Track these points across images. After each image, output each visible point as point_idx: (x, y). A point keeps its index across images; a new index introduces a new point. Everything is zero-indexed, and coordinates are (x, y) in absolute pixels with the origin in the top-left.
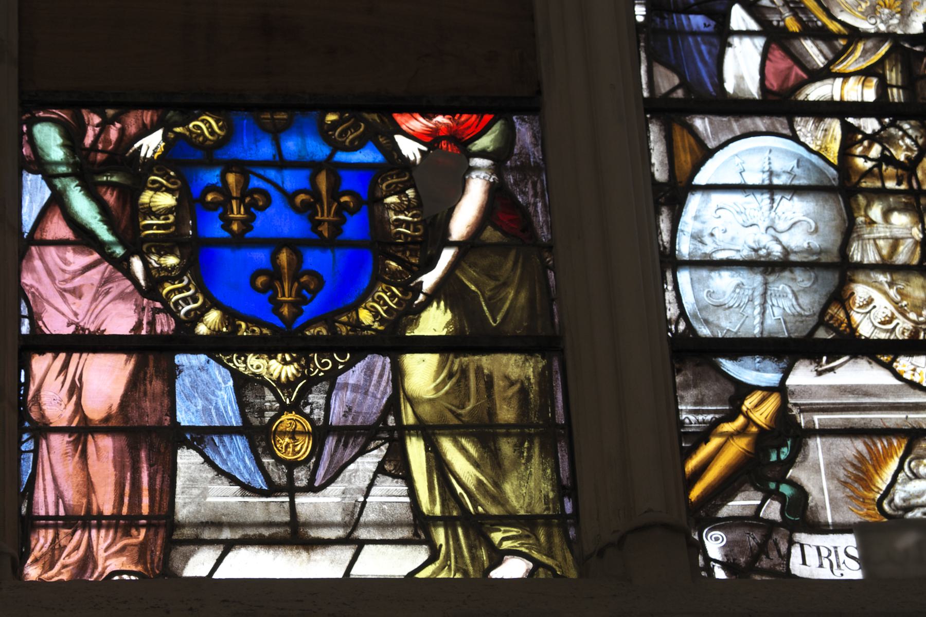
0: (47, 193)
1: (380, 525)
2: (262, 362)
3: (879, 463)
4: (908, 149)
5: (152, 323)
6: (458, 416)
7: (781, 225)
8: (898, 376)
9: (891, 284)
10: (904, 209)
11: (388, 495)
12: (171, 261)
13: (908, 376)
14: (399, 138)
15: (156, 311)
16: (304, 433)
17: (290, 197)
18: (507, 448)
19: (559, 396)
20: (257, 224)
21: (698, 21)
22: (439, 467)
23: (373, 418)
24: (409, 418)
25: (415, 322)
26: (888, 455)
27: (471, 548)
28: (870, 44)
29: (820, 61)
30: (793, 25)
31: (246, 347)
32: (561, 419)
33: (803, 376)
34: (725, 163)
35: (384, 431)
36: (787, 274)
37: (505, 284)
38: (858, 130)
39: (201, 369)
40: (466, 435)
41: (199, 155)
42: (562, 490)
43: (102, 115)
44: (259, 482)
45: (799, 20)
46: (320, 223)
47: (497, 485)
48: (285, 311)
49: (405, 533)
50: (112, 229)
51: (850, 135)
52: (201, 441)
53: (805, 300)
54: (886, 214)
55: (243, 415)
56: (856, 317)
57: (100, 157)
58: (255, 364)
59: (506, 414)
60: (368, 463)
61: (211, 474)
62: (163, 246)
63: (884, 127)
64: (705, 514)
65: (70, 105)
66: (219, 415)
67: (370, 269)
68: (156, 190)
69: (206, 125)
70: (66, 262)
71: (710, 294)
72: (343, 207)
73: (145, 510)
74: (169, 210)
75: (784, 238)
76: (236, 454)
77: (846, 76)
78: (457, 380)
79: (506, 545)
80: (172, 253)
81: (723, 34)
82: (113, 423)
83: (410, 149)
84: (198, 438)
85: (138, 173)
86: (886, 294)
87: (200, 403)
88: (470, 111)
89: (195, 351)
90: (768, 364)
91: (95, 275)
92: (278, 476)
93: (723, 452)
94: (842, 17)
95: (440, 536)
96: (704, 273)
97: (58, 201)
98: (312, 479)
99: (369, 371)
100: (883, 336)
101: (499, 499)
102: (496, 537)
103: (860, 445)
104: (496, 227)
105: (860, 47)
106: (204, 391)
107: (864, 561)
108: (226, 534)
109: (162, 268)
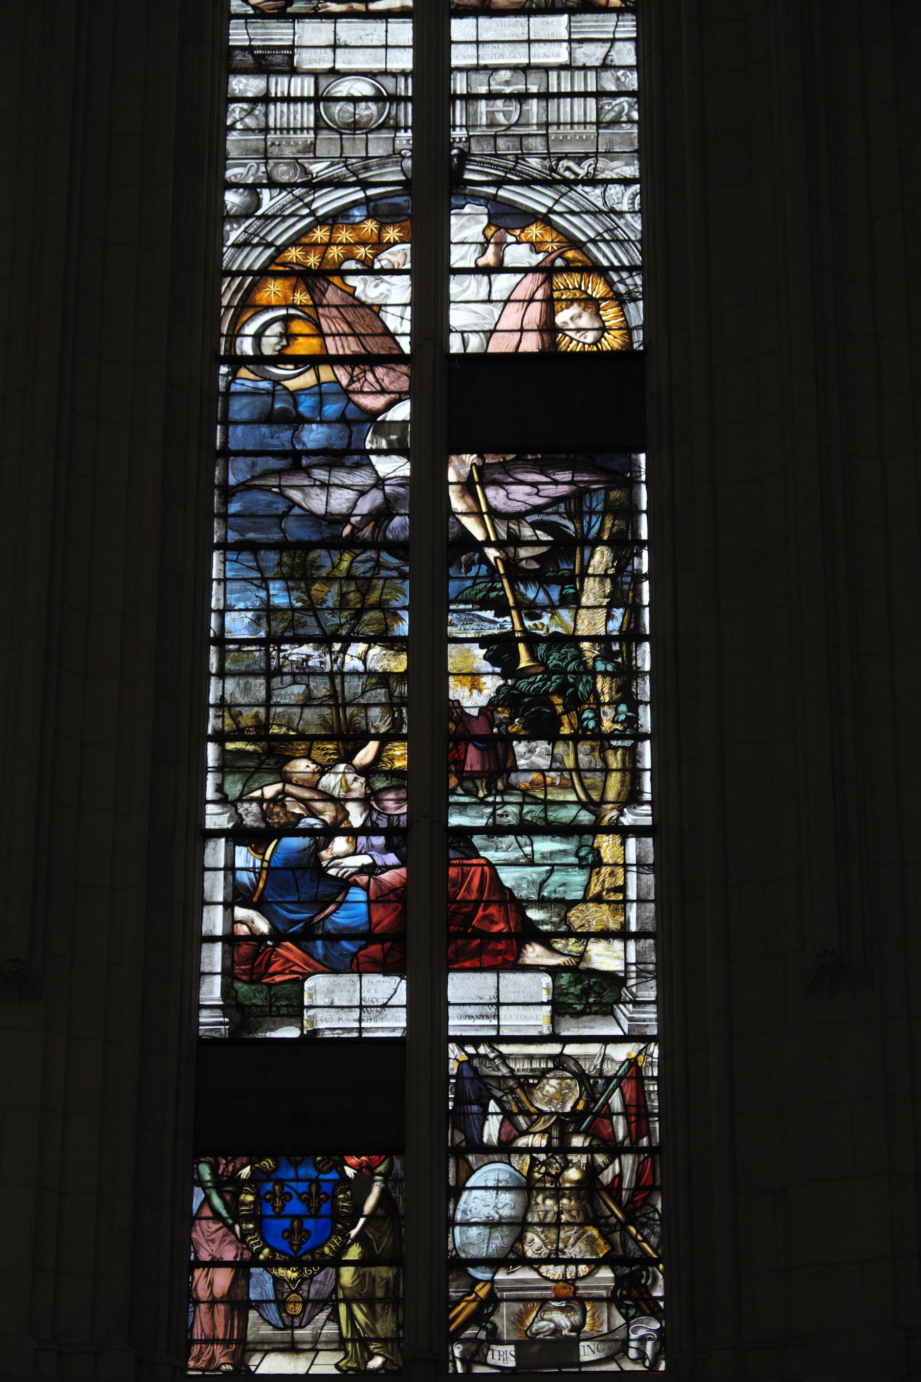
0: (203, 1196)
1: (326, 1342)
2: (284, 1271)
3: (528, 1313)
4: (557, 1169)
5: (242, 1254)
6: (360, 1295)
7: (500, 1206)
8: (540, 1274)
9: (542, 1232)
10: (550, 1198)
11: (330, 1330)
12: (251, 1226)
13: (544, 1274)
14: (346, 1168)
15: (244, 1249)
16: (299, 1302)
17: (300, 1195)
18: (379, 1308)
19: (401, 1286)
20: (286, 1208)
21: (475, 1108)
22: (351, 1316)
23: (327, 1296)
24: (341, 1296)
25: (346, 1253)
26: (532, 1310)
27: (361, 1352)
28: (547, 1117)
29: (525, 1126)
30: (515, 1110)
31: (278, 1265)
32: (401, 1296)
33: (501, 1276)
34: (480, 1177)
35: (329, 1302)
36: (500, 1228)
37: (384, 1235)
38: (537, 1159)
39: (261, 1274)
40: (362, 1303)
41: (264, 1176)
42: (399, 1327)
43: (226, 1159)
44: (280, 1324)
45: (518, 1107)
46: (311, 1207)
47: (374, 1325)
48: (295, 1248)
49: (335, 1346)
50: (228, 1212)
51: (533, 1160)
52: (258, 1307)
53: (506, 1240)
54: (544, 1200)
55: (276, 1294)
56: (526, 1248)
57: (225, 1179)
58: (281, 1272)
59: (380, 1293)
60: (323, 1316)
61: (261, 1321)
62: (248, 1219)
63: (548, 1158)
64: (454, 1338)
65: (213, 1153)
66: (266, 1295)
67: (330, 1228)
68: (246, 1194)
69: (268, 1163)
70: (209, 1228)
71: (467, 1238)
72: (321, 1200)
73: (235, 1337)
74: (251, 1203)
75: (500, 1211)
76: (271, 1311)
77: (535, 1133)
78: (360, 1278)
79: (375, 1351)
80: (251, 1223)
81: (485, 1114)
82: (225, 1299)
83: (350, 1172)
84: (258, 1305)
85: (239, 1185)
86: (539, 1237)
87: (259, 1290)
88: (376, 1155)
89: (258, 1267)
90: (488, 1270)
91: (220, 1233)
92: (288, 1322)
93: (465, 1309)
94: (537, 1105)
95: (350, 1347)
96: (465, 1228)
97: (207, 1200)
98: (301, 1323)
99: (326, 1275)
100: (536, 1256)
101: (374, 1331)
102: (372, 1347)
103: (521, 1306)
104: (382, 1209)
105: (543, 1119)
106: (261, 1285)
107: (517, 1357)
108: (266, 1347)
109: (247, 1229)
